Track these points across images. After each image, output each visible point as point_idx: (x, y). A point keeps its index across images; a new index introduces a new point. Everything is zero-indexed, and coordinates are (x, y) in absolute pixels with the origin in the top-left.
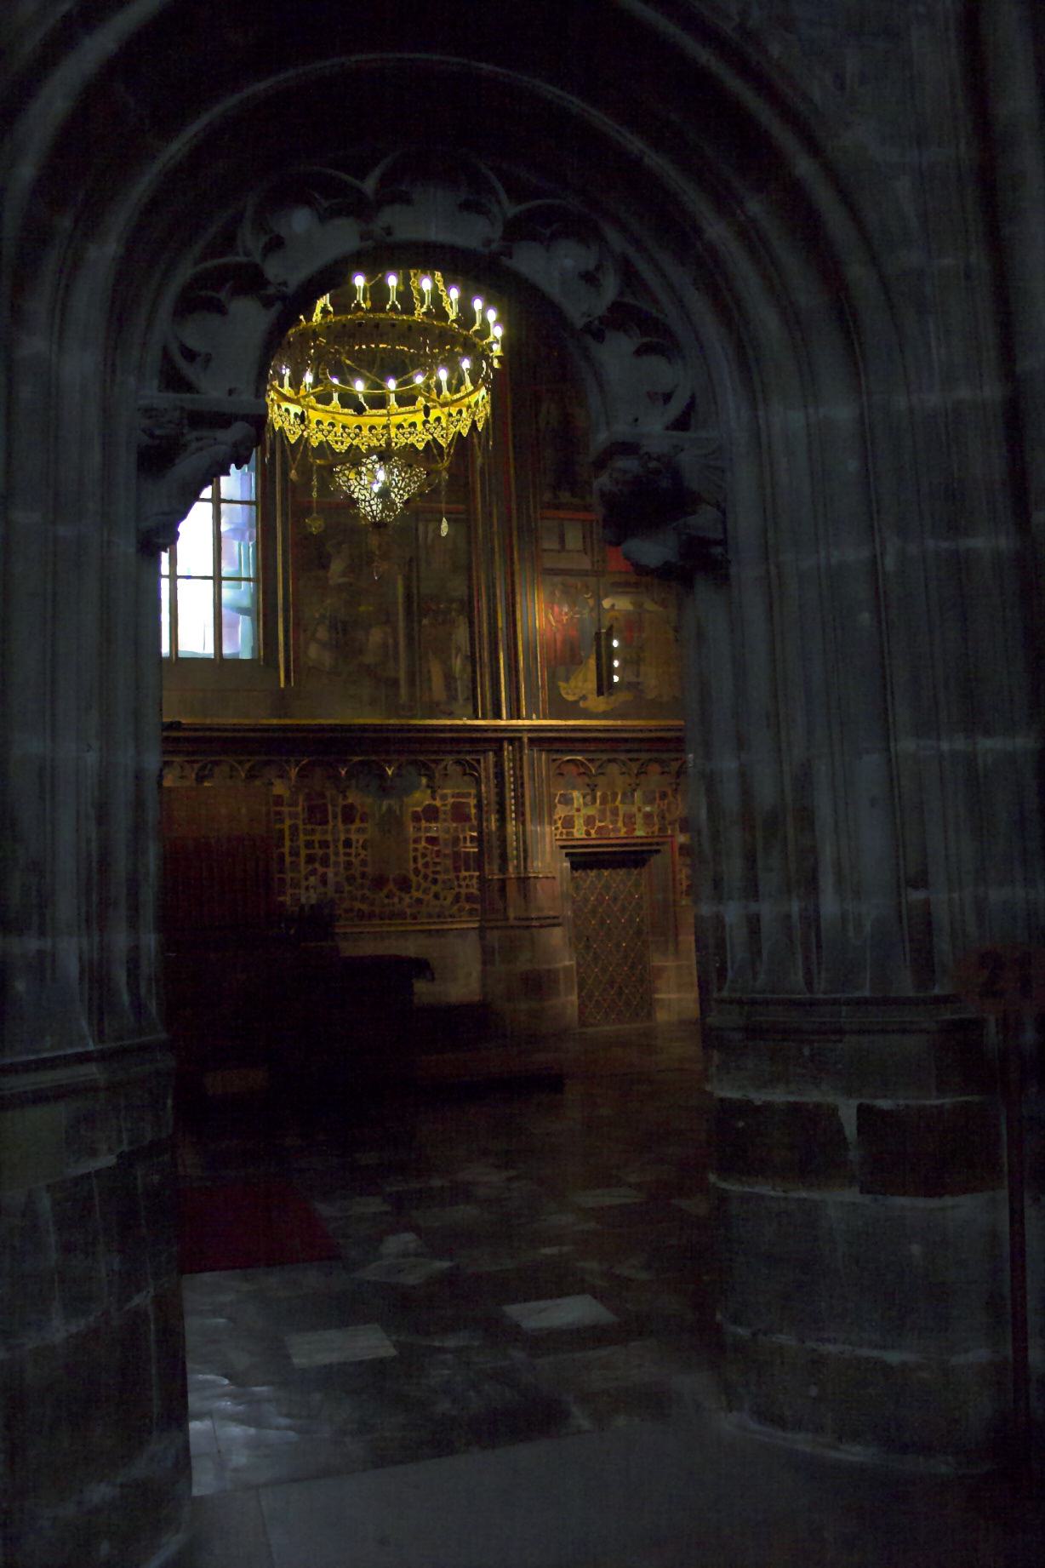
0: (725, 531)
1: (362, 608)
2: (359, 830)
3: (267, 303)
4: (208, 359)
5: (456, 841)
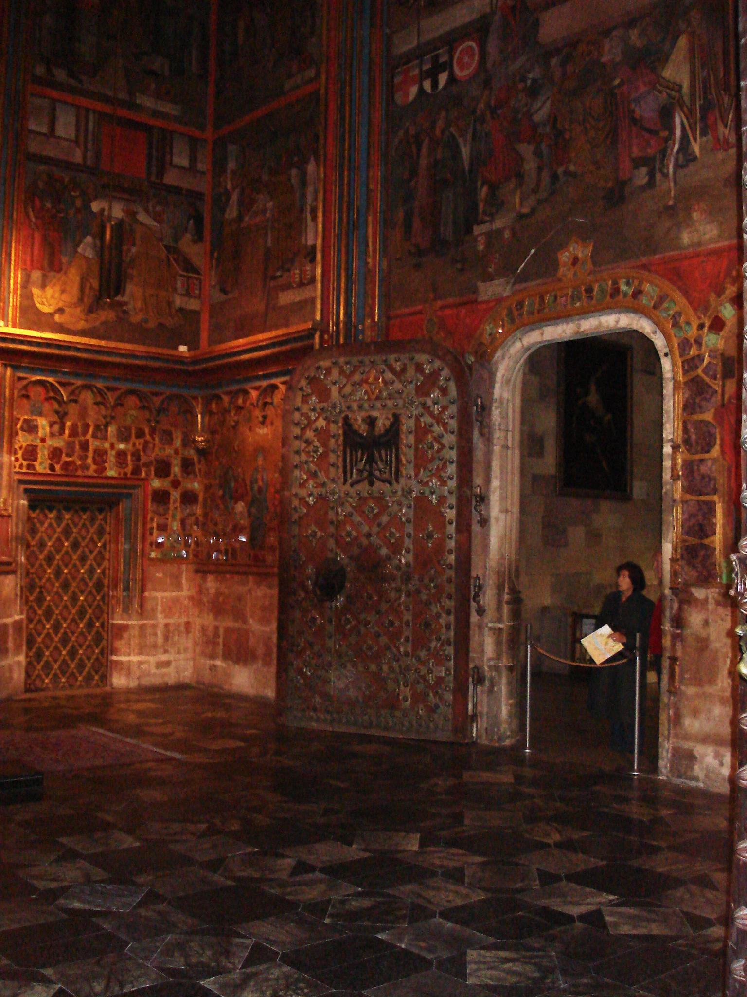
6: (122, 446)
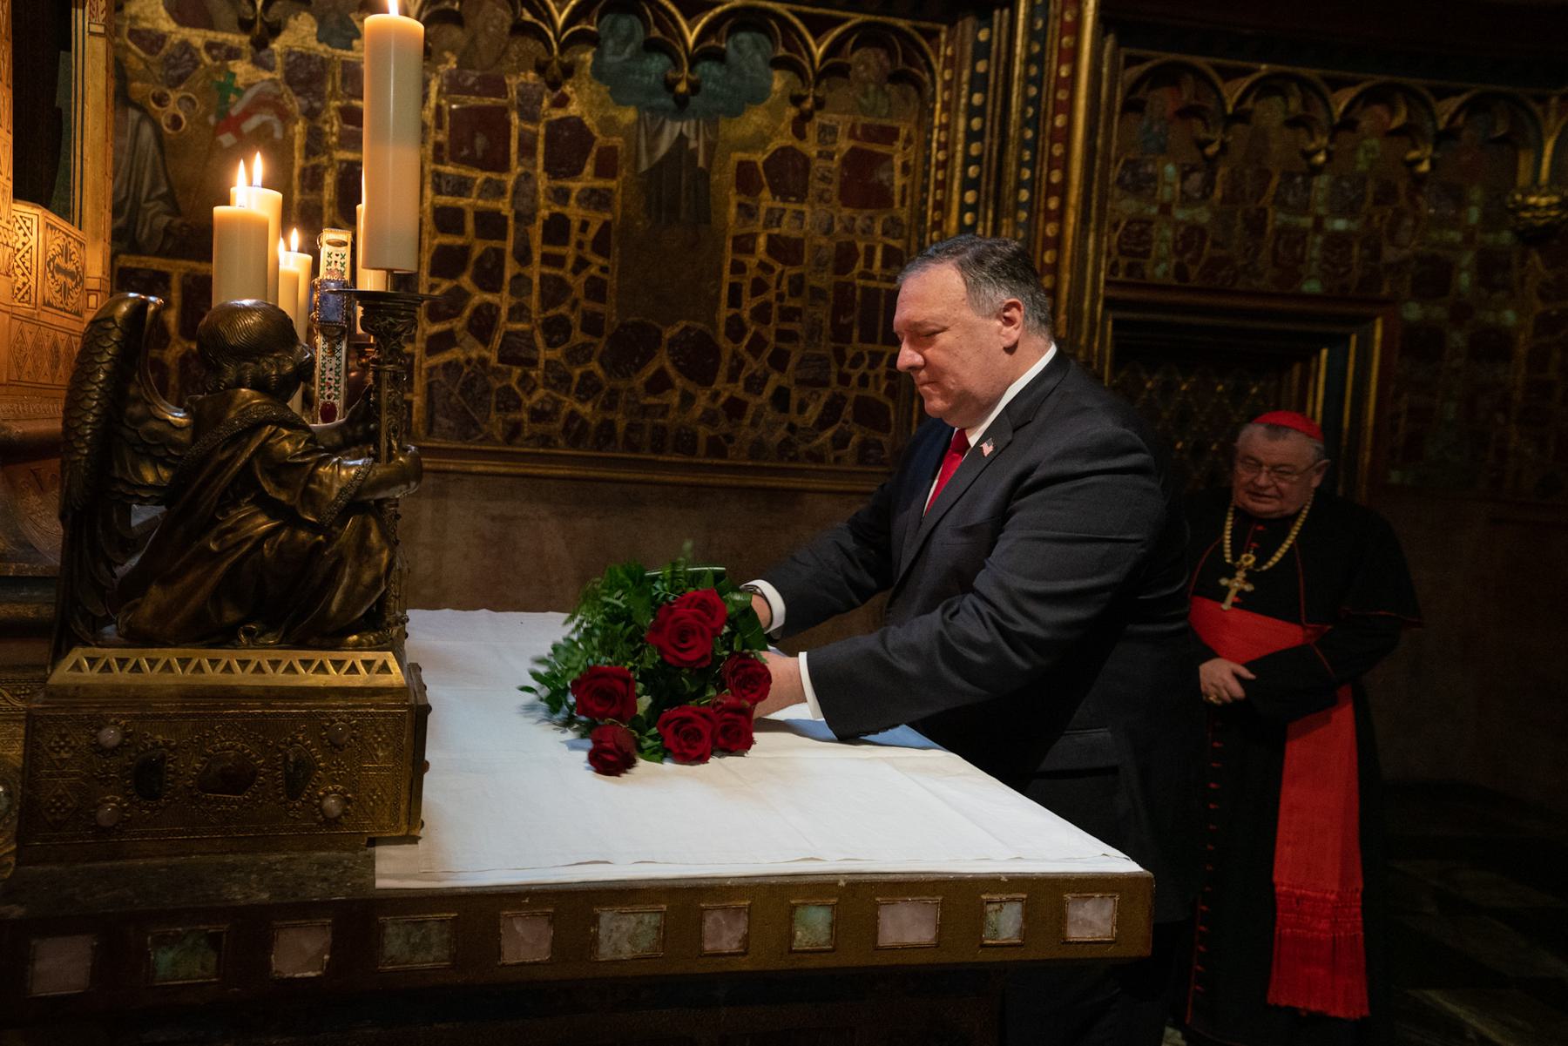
5: (845, 257)
6: (1340, 224)
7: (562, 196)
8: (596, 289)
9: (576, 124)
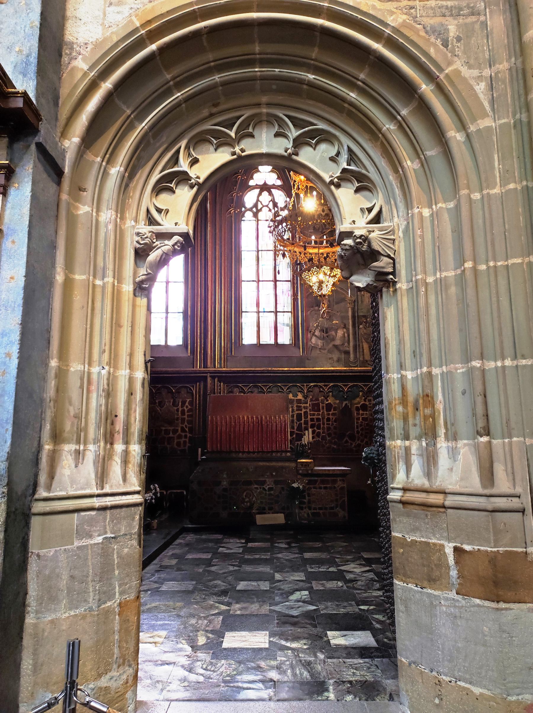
0: (394, 267)
1: (334, 322)
2: (333, 414)
3: (192, 187)
4: (167, 211)
7: (329, 414)
8: (335, 428)
9: (330, 403)
